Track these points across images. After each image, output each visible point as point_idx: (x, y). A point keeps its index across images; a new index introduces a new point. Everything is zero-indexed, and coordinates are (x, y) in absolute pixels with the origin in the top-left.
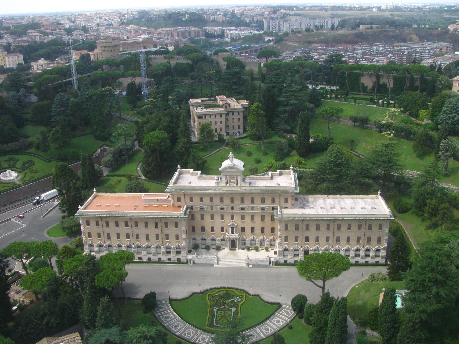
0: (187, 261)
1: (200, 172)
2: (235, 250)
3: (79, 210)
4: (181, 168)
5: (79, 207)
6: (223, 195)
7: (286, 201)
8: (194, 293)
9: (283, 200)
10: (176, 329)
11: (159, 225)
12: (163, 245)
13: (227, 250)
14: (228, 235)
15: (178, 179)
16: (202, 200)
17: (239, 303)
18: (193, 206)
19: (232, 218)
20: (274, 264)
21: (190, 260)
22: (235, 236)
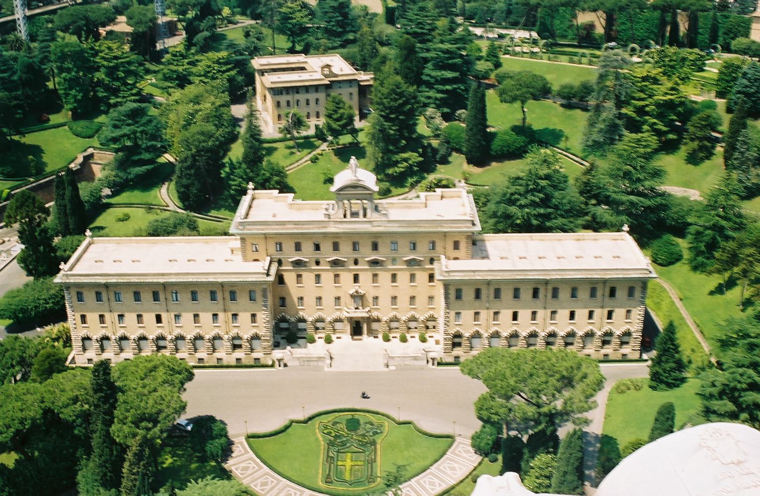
0: (274, 362)
1: (291, 195)
2: (361, 340)
3: (62, 272)
4: (254, 189)
5: (61, 267)
6: (339, 237)
7: (456, 246)
8: (292, 422)
9: (450, 245)
10: (262, 490)
11: (219, 296)
12: (227, 333)
13: (347, 337)
14: (350, 311)
15: (250, 207)
16: (298, 247)
17: (376, 437)
18: (283, 260)
19: (356, 279)
20: (436, 363)
21: (279, 360)
22: (361, 313)
